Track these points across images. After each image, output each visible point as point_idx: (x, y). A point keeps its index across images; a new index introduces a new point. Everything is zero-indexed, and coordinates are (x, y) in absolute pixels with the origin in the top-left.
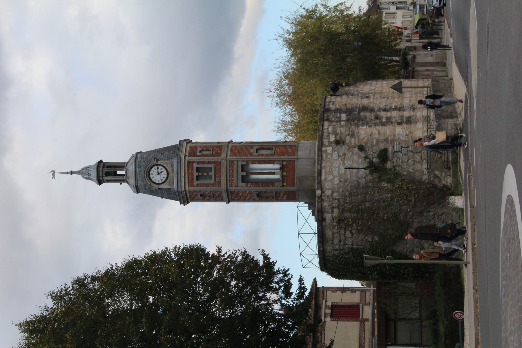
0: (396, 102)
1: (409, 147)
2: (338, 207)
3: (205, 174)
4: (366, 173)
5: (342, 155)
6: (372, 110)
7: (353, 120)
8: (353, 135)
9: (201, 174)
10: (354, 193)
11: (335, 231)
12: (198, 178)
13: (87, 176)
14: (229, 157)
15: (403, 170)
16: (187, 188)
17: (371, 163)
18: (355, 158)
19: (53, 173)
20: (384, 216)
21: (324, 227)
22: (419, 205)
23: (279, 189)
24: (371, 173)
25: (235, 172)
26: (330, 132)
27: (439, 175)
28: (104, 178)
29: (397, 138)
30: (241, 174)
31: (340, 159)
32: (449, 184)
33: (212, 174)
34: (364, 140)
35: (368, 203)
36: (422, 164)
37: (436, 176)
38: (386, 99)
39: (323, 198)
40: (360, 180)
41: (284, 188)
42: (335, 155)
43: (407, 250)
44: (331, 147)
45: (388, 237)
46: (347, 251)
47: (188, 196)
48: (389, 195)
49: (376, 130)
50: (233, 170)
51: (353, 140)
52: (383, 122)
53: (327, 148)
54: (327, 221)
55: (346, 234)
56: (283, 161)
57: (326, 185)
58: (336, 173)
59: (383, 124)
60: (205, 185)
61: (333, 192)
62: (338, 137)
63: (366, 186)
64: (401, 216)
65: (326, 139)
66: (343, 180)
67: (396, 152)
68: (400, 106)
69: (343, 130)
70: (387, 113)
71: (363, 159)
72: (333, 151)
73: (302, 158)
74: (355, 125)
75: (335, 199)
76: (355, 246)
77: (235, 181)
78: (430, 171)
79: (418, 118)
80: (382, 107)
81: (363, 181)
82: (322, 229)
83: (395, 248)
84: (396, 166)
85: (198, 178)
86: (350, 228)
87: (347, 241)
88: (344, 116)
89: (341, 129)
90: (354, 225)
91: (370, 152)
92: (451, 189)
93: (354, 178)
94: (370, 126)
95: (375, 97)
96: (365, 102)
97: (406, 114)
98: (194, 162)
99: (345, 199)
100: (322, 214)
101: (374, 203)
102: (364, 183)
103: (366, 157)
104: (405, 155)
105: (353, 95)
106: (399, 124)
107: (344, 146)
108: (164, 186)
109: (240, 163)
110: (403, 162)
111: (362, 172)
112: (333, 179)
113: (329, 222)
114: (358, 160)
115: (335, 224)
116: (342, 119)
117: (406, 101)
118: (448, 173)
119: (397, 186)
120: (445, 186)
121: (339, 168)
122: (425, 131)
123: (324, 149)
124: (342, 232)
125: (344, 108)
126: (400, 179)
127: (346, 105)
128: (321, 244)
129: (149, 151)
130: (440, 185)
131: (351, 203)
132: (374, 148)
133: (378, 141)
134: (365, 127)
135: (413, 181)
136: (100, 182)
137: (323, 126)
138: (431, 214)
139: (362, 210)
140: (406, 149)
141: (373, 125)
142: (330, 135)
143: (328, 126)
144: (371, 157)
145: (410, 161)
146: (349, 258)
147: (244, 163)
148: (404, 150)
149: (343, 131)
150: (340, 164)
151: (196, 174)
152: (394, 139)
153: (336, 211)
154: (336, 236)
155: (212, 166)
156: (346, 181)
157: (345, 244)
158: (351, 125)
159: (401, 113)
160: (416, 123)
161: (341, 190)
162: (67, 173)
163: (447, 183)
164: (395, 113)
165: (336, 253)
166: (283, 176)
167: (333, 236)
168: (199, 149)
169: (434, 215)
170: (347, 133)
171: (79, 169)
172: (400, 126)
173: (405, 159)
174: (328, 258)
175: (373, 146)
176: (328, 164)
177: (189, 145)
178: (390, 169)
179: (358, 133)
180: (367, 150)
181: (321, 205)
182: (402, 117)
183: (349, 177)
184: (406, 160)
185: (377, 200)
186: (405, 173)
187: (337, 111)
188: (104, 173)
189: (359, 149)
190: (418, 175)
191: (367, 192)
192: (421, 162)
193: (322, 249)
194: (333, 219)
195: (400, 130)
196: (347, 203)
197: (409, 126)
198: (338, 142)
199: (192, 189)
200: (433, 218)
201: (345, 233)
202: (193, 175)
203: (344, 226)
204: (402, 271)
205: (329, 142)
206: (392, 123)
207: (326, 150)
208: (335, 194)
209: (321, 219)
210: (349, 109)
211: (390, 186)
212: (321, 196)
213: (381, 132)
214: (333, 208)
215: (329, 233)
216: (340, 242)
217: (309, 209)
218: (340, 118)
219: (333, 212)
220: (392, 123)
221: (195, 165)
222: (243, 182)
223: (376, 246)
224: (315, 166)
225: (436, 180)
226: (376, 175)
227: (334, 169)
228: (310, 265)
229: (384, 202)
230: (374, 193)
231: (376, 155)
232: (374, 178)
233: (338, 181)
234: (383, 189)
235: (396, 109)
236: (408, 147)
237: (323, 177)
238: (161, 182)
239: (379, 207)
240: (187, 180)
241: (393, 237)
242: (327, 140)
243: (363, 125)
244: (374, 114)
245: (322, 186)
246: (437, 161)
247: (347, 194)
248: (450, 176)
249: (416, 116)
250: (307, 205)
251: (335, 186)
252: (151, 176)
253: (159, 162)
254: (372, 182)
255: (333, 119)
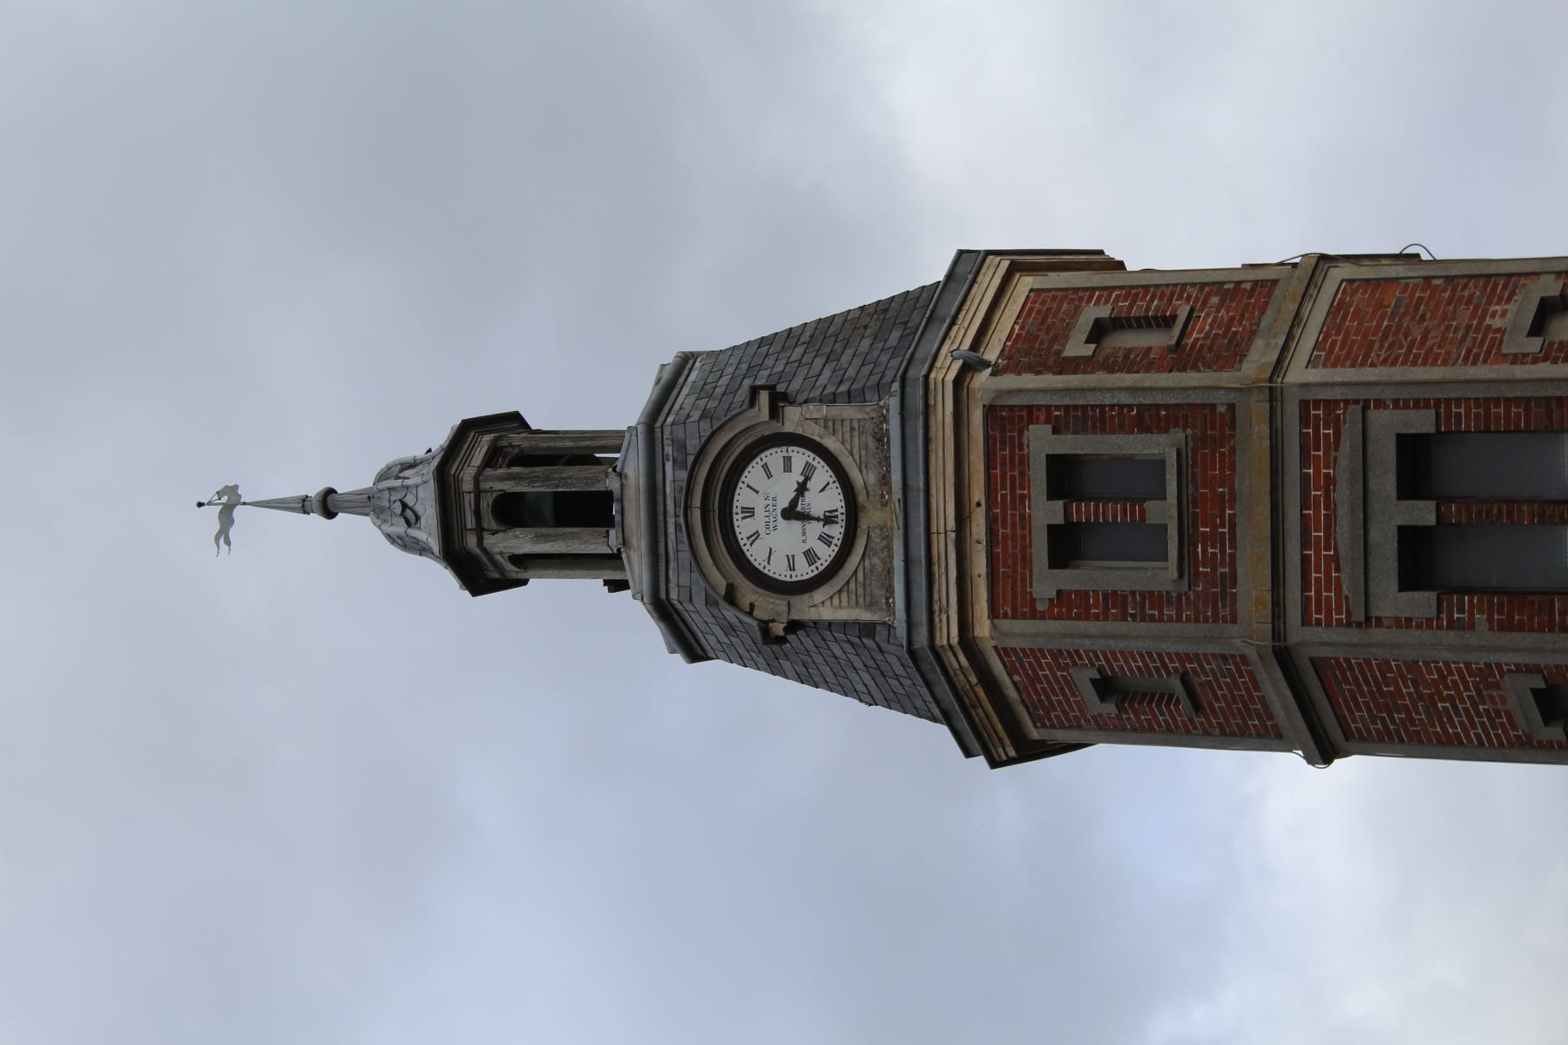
3: (1114, 511)
9: (1083, 512)
12: (1066, 545)
13: (400, 528)
14: (1298, 373)
16: (983, 628)
19: (229, 502)
25: (1344, 494)
28: (489, 540)
30: (1398, 512)
33: (1164, 511)
47: (1012, 693)
50: (1330, 481)
60: (1116, 603)
77: (1348, 579)
85: (1066, 545)
98: (1030, 414)
108: (823, 607)
109: (1386, 425)
129: (762, 342)
136: (479, 577)
147: (1422, 422)
151: (1045, 512)
155: (1162, 446)
162: (303, 505)
168: (1093, 312)
171: (365, 481)
177: (1025, 284)
188: (487, 502)
199: (1022, 632)
202: (1025, 520)
221: (1041, 442)
222: (1409, 581)
238: (804, 571)
240: (979, 565)
252: (743, 528)
253: (793, 419)
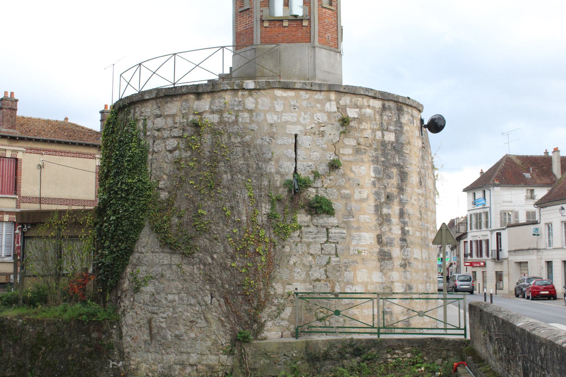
0: (414, 233)
1: (337, 256)
2: (221, 122)
4: (287, 175)
5: (322, 129)
6: (401, 190)
7: (384, 154)
8: (357, 151)
10: (249, 151)
11: (178, 119)
15: (293, 246)
17: (304, 184)
18: (316, 155)
20: (203, 209)
21: (185, 97)
22: (225, 276)
23: (257, 15)
24: (288, 184)
26: (363, 110)
27: (282, 315)
29: (355, 234)
31: (313, 125)
32: (265, 334)
34: (348, 172)
35: (229, 177)
36: (304, 281)
37: (281, 309)
38: (419, 216)
39: (240, 93)
40: (273, 163)
41: (259, 23)
42: (323, 118)
43: (142, 253)
44: (336, 109)
45: (165, 218)
46: (142, 143)
48: (244, 218)
49: (368, 195)
51: (349, 151)
52: (381, 208)
53: (334, 103)
54: (197, 103)
55: (172, 140)
56: (309, 20)
57: (265, 99)
58: (287, 117)
59: (378, 208)
61: (250, 111)
62: (352, 124)
63: (262, 175)
64: (203, 241)
65: (351, 101)
66: (274, 130)
67: (328, 232)
68: (408, 242)
69: (368, 133)
70: (397, 216)
71: (314, 169)
72: (329, 114)
73: (314, 55)
74: (377, 157)
75: (237, 116)
76: (150, 157)
78: (291, 298)
79: (389, 273)
80: (406, 207)
81: (271, 168)
82: (182, 94)
83: (146, 230)
84: (301, 232)
86: (182, 146)
87: (159, 141)
88: (390, 137)
89: (369, 131)
90: (189, 153)
91: (327, 183)
92: (256, 338)
93: (277, 152)
94: (374, 184)
95: (420, 197)
96: (414, 179)
97: (396, 252)
99: (237, 134)
100: (208, 93)
101: (228, 188)
102: (268, 170)
103: (317, 175)
104: (322, 249)
105: (423, 158)
106: (379, 239)
107: (338, 133)
110: (309, 245)
111: (288, 167)
112: (276, 113)
113: (195, 107)
114: (311, 160)
115: (191, 118)
116: (385, 133)
117: (416, 253)
118: (286, 333)
119: (262, 232)
120: (262, 326)
121: (297, 123)
122: (366, 287)
123: (333, 96)
124: (176, 132)
125: (403, 139)
126: (275, 239)
127: (409, 143)
128: (154, 95)
130: (264, 316)
131: (231, 145)
132: (335, 191)
133: (347, 198)
134: (373, 174)
135: (271, 264)
137: (374, 98)
138: (208, 299)
139: (215, 167)
140: (333, 252)
141: (376, 189)
142: (357, 110)
143: (373, 108)
144: (318, 184)
145: (310, 258)
146: (130, 149)
148: (330, 248)
149: (368, 133)
150: (305, 126)
152: (353, 228)
153: (215, 118)
154: (170, 121)
156: (272, 136)
157: (155, 139)
158: (376, 150)
159: (397, 242)
160: (381, 271)
161: (254, 126)
163: (268, 330)
164: (396, 231)
165: (140, 125)
166: (281, 20)
167: (168, 116)
169: (206, 305)
170: (362, 140)
172: (376, 239)
173: (315, 249)
174: (132, 111)
175: (339, 188)
176: (304, 103)
178: (294, 220)
179: (362, 161)
180: (332, 177)
181: (227, 90)
182: (390, 243)
183: (280, 142)
184: (312, 251)
185: (235, 196)
186: (287, 249)
187: (399, 124)
189: (334, 161)
190: (282, 273)
191: (249, 177)
192: (307, 279)
193: (147, 97)
194: (200, 114)
195: (367, 239)
196: (230, 137)
197: (375, 257)
198: (345, 121)
200: (199, 304)
201: (174, 137)
203: (186, 135)
204: (107, 243)
205: (346, 106)
206: (381, 225)
207: (330, 100)
208: (246, 115)
209: (200, 91)
210: (402, 147)
211: (261, 219)
212: (244, 89)
213: (364, 205)
214: (220, 112)
215: (173, 107)
216: (158, 130)
217: (220, 76)
218: (387, 130)
219: (212, 112)
220: (381, 225)
223: (149, 196)
224: (300, 79)
225: (274, 308)
226: (283, 193)
227: (295, 114)
228: (124, 84)
229: (232, 208)
230: (248, 189)
231: (321, 193)
232: (277, 188)
233: (272, 122)
234: (257, 206)
235: (404, 232)
236: (337, 255)
237: (279, 93)
239: (221, 199)
241: (166, 226)
242: (348, 102)
243: (376, 171)
244: (396, 193)
245: (262, 92)
246: (310, 310)
247: (247, 138)
248: (282, 337)
249: (392, 270)
250: (227, 71)
251: (262, 115)
254: (269, 186)
255: (385, 117)
